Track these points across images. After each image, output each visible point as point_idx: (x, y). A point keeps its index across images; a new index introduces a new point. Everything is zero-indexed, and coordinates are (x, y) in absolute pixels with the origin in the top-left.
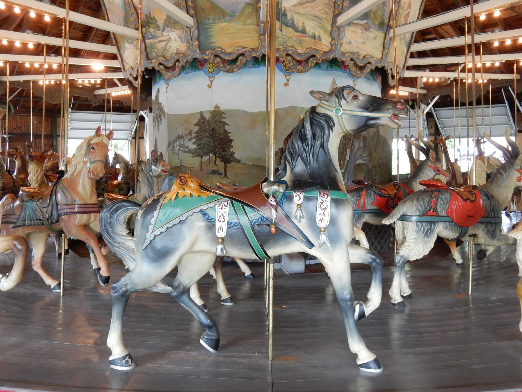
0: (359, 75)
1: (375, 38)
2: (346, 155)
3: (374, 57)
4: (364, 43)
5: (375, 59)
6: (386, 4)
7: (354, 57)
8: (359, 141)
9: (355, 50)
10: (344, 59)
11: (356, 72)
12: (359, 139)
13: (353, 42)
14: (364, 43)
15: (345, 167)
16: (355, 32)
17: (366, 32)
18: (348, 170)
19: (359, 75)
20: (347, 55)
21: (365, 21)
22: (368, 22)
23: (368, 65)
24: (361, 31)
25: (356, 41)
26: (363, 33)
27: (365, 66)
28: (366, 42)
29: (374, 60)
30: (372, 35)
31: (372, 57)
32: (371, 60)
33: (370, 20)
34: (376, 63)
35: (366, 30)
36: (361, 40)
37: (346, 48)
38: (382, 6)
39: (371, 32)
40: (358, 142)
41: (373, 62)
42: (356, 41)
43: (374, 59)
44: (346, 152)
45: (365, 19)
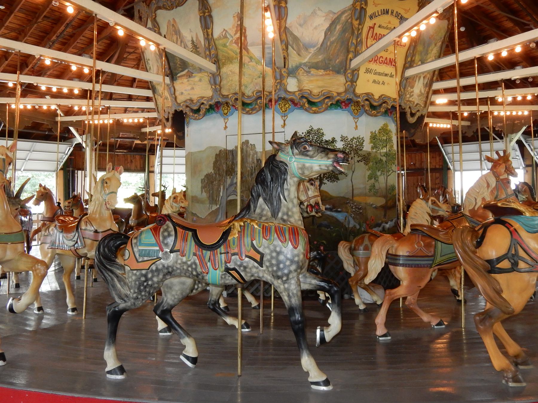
0: (197, 118)
1: (200, 80)
2: (220, 191)
3: (204, 97)
4: (193, 88)
5: (206, 98)
6: (198, 46)
7: (187, 104)
8: (231, 177)
9: (188, 98)
10: (181, 109)
11: (194, 116)
12: (232, 175)
13: (184, 92)
14: (193, 88)
15: (220, 203)
16: (182, 83)
17: (191, 79)
18: (221, 205)
19: (197, 118)
20: (181, 105)
21: (187, 71)
22: (189, 70)
23: (202, 106)
24: (186, 80)
25: (186, 90)
26: (188, 81)
27: (200, 107)
28: (194, 87)
29: (205, 100)
30: (197, 79)
31: (203, 98)
32: (202, 101)
33: (190, 68)
34: (208, 101)
35: (190, 77)
36: (189, 88)
37: (181, 99)
38: (196, 50)
39: (195, 76)
40: (230, 178)
41: (205, 102)
42: (186, 90)
43: (204, 99)
44: (221, 189)
45: (185, 69)
